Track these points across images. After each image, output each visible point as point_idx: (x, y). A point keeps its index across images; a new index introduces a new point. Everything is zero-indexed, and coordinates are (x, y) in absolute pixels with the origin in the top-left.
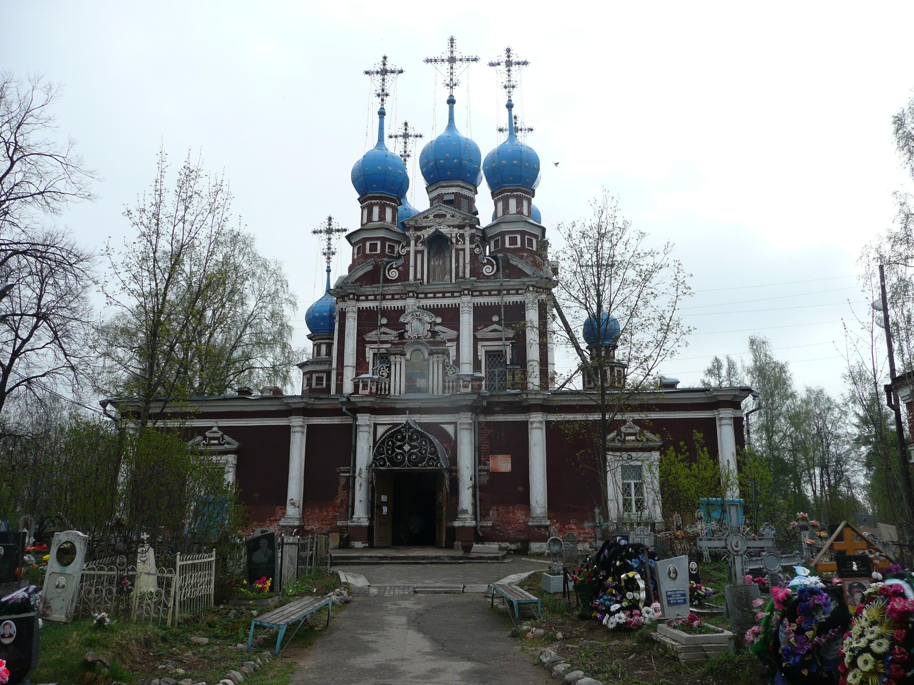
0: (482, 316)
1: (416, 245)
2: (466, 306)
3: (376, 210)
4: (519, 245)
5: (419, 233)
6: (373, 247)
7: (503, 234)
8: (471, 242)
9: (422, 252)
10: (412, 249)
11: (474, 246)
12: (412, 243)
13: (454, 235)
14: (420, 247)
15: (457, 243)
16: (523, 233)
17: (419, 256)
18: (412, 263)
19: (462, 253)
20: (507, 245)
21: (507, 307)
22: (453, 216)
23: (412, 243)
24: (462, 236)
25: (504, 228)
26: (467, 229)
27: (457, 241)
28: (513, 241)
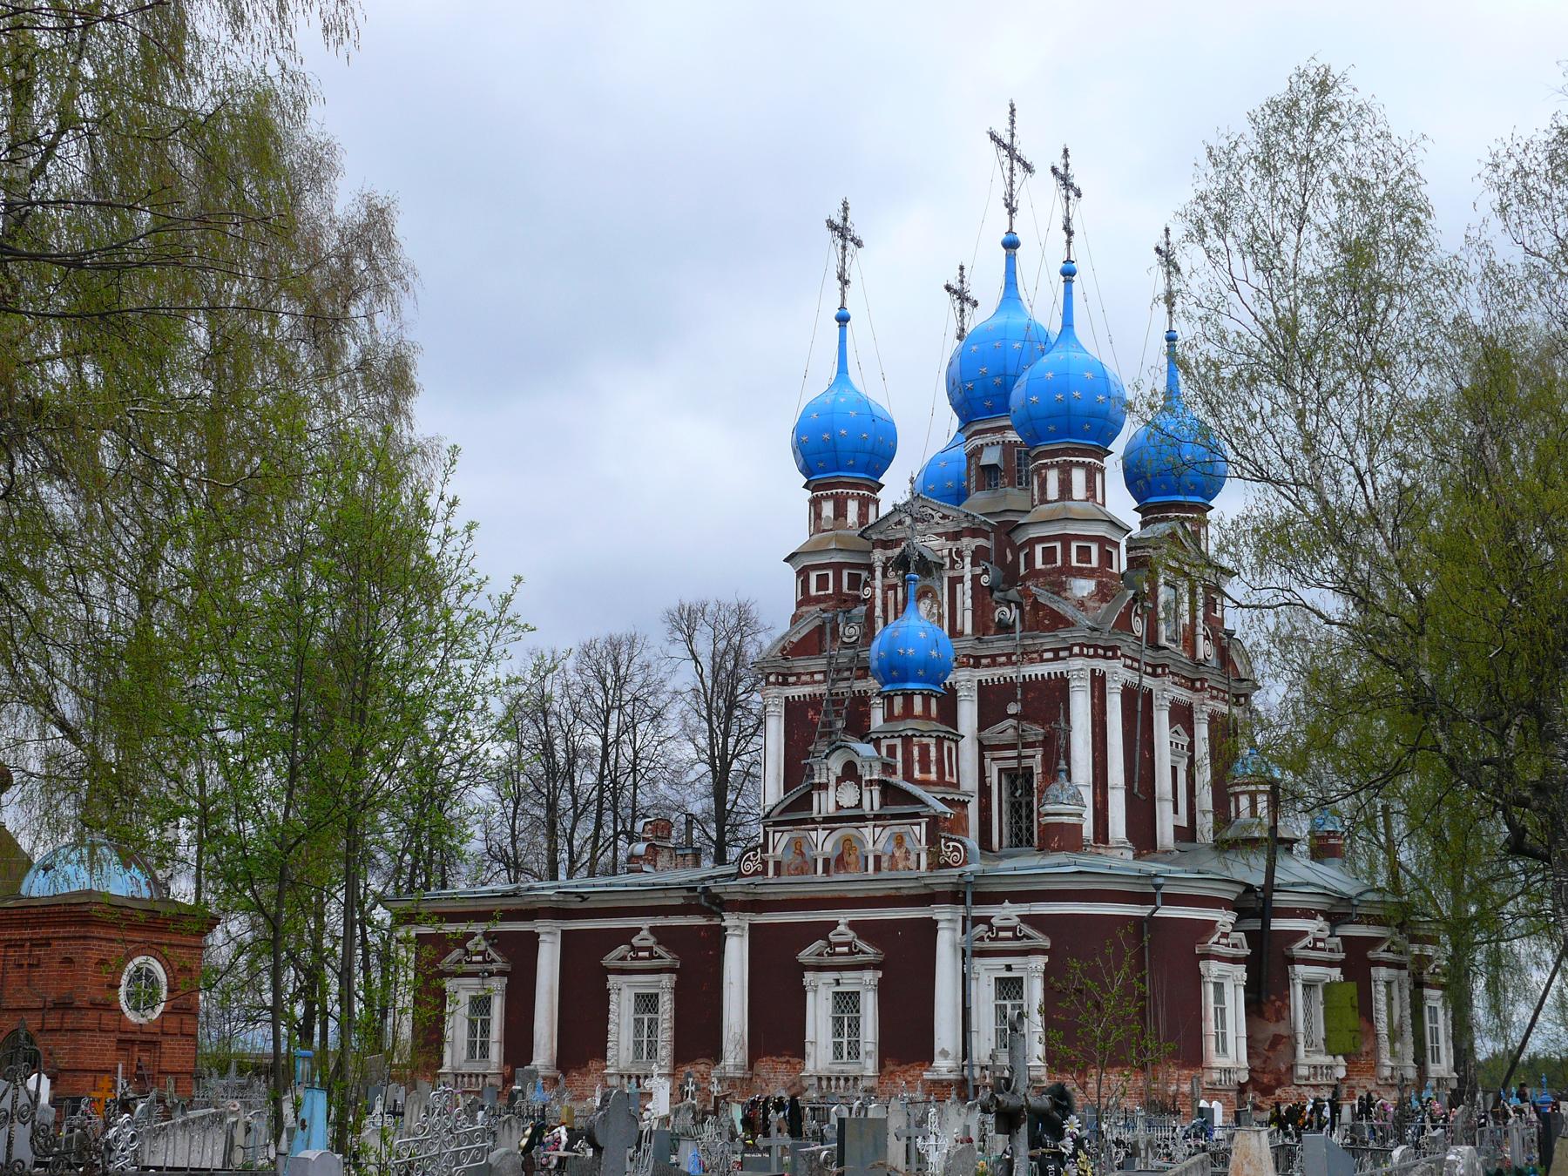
0: (992, 702)
1: (884, 575)
2: (966, 681)
3: (828, 509)
4: (1059, 563)
5: (889, 553)
6: (822, 582)
7: (1032, 542)
8: (974, 564)
9: (894, 587)
10: (878, 583)
11: (978, 571)
12: (878, 574)
13: (946, 552)
14: (893, 578)
15: (952, 568)
16: (1066, 540)
17: (891, 593)
18: (878, 611)
19: (959, 586)
20: (1039, 564)
21: (1030, 685)
22: (944, 517)
23: (878, 574)
24: (959, 553)
25: (1034, 533)
26: (965, 541)
27: (953, 562)
28: (1049, 555)
